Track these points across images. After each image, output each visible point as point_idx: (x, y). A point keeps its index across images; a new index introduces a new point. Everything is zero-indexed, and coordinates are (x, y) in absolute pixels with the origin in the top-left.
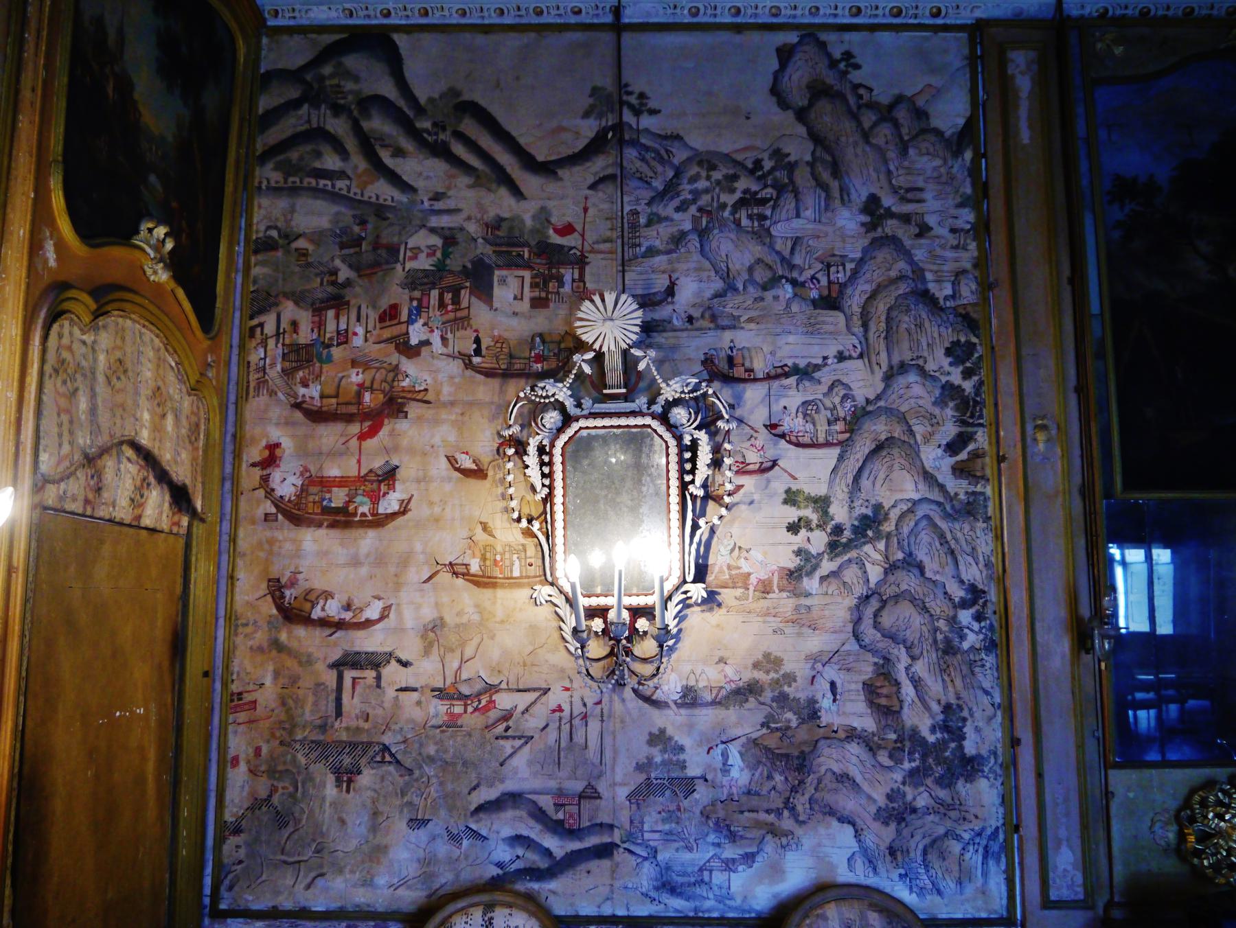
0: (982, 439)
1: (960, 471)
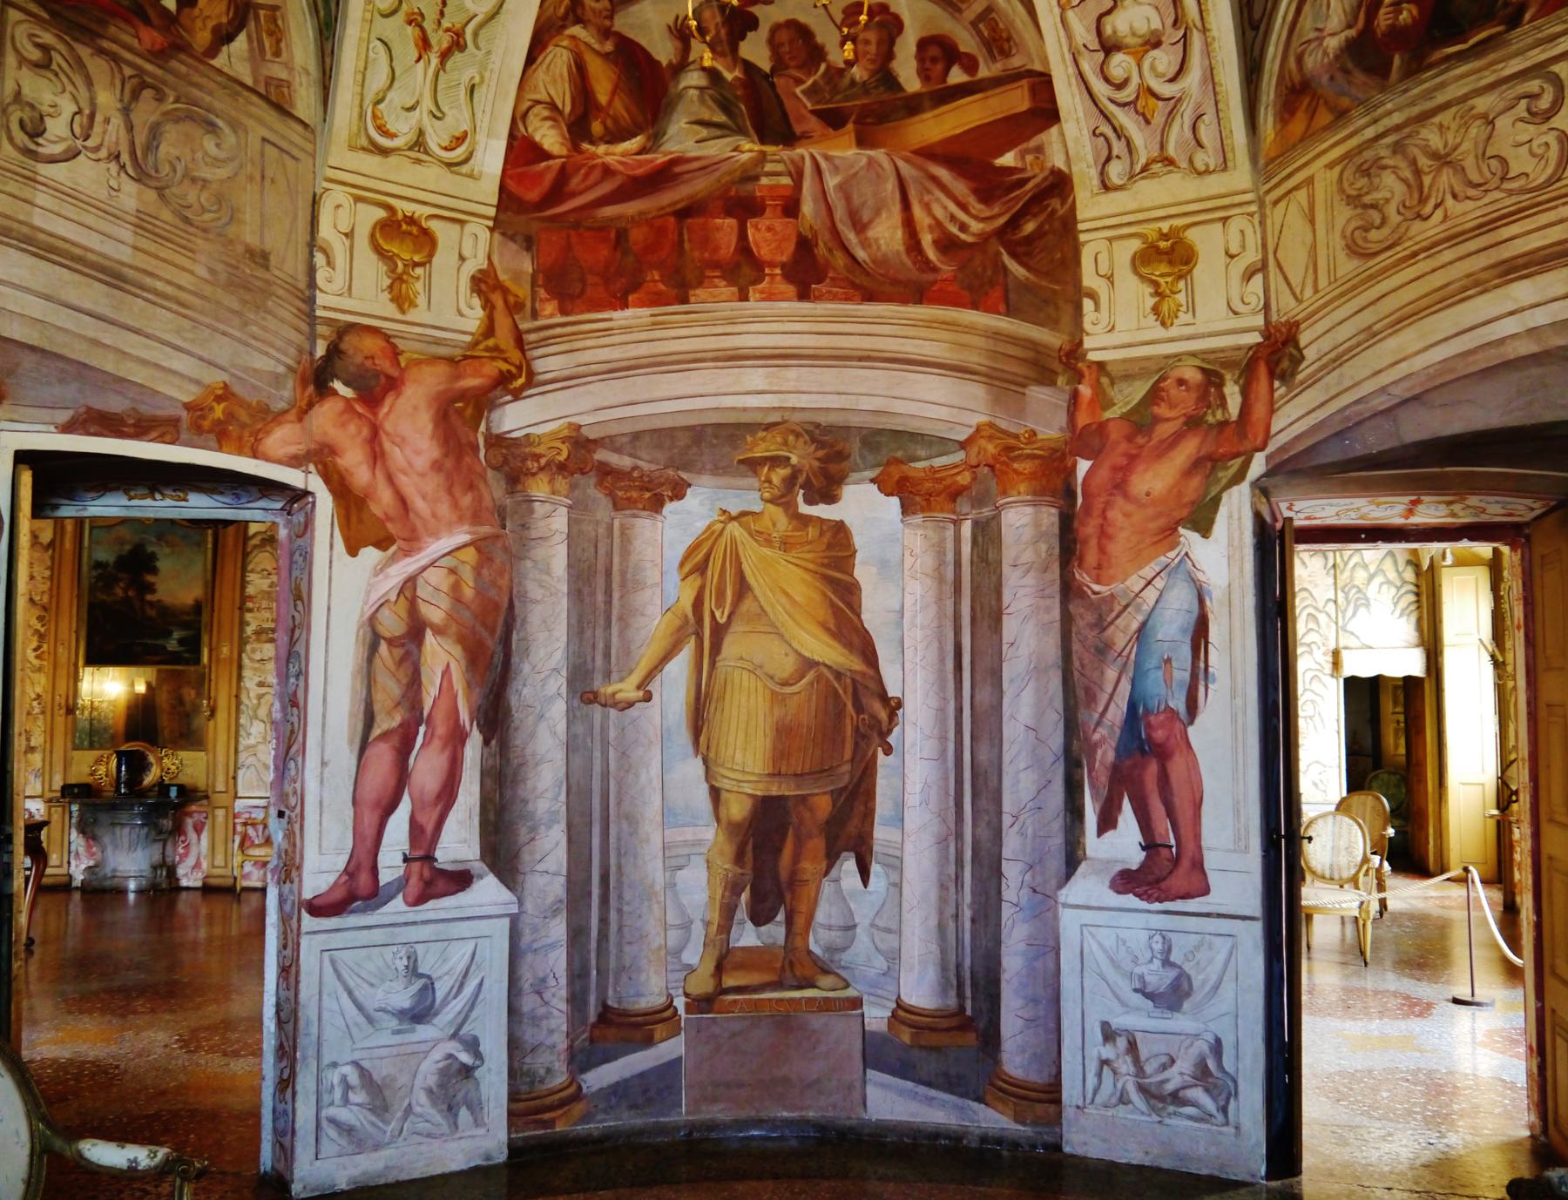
0: (45, 647)
1: (37, 657)
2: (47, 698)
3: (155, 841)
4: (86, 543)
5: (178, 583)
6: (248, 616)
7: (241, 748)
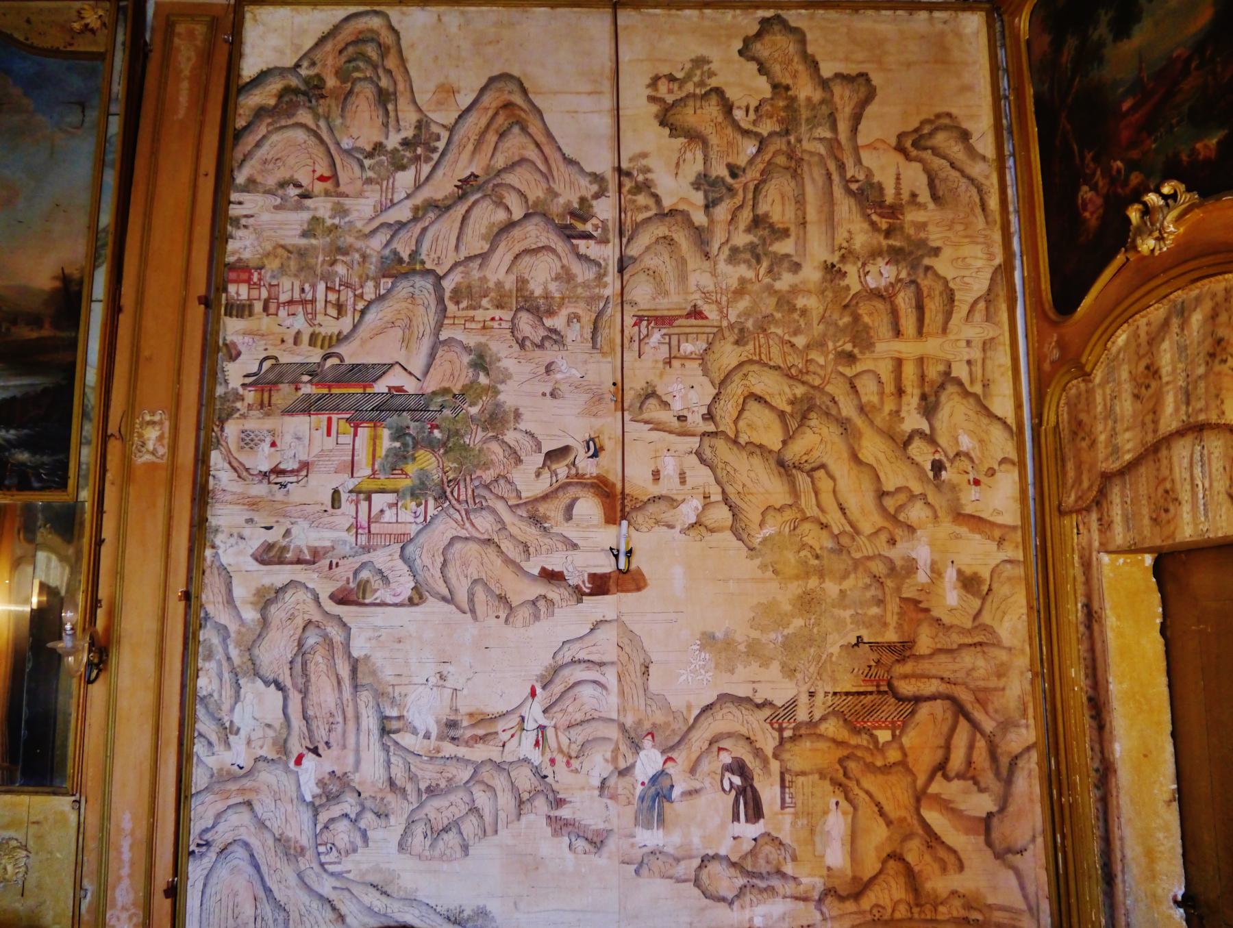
6: (233, 329)
7: (199, 778)
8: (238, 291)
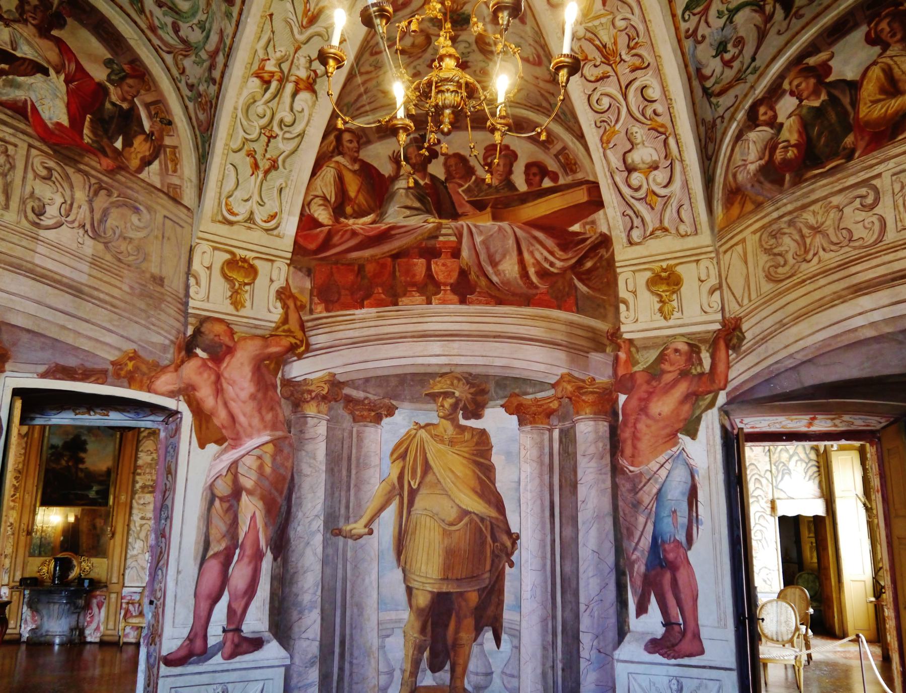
0: (18, 495)
1: (13, 501)
2: (16, 525)
3: (73, 613)
4: (47, 434)
5: (98, 459)
6: (138, 478)
7: (128, 556)
8: (139, 471)
